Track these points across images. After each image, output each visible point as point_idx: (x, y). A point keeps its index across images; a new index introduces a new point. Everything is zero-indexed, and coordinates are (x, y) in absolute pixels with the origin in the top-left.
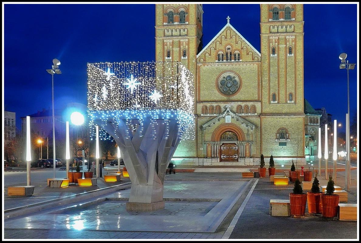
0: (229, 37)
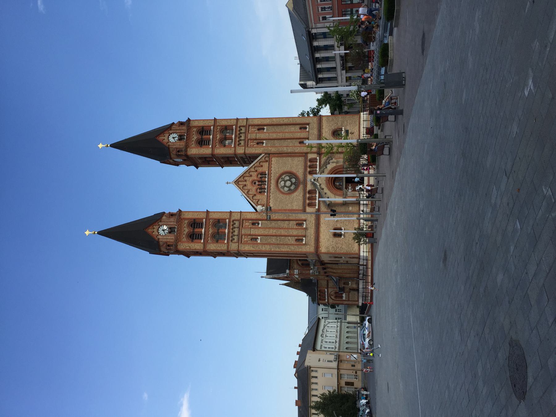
0: (245, 183)
